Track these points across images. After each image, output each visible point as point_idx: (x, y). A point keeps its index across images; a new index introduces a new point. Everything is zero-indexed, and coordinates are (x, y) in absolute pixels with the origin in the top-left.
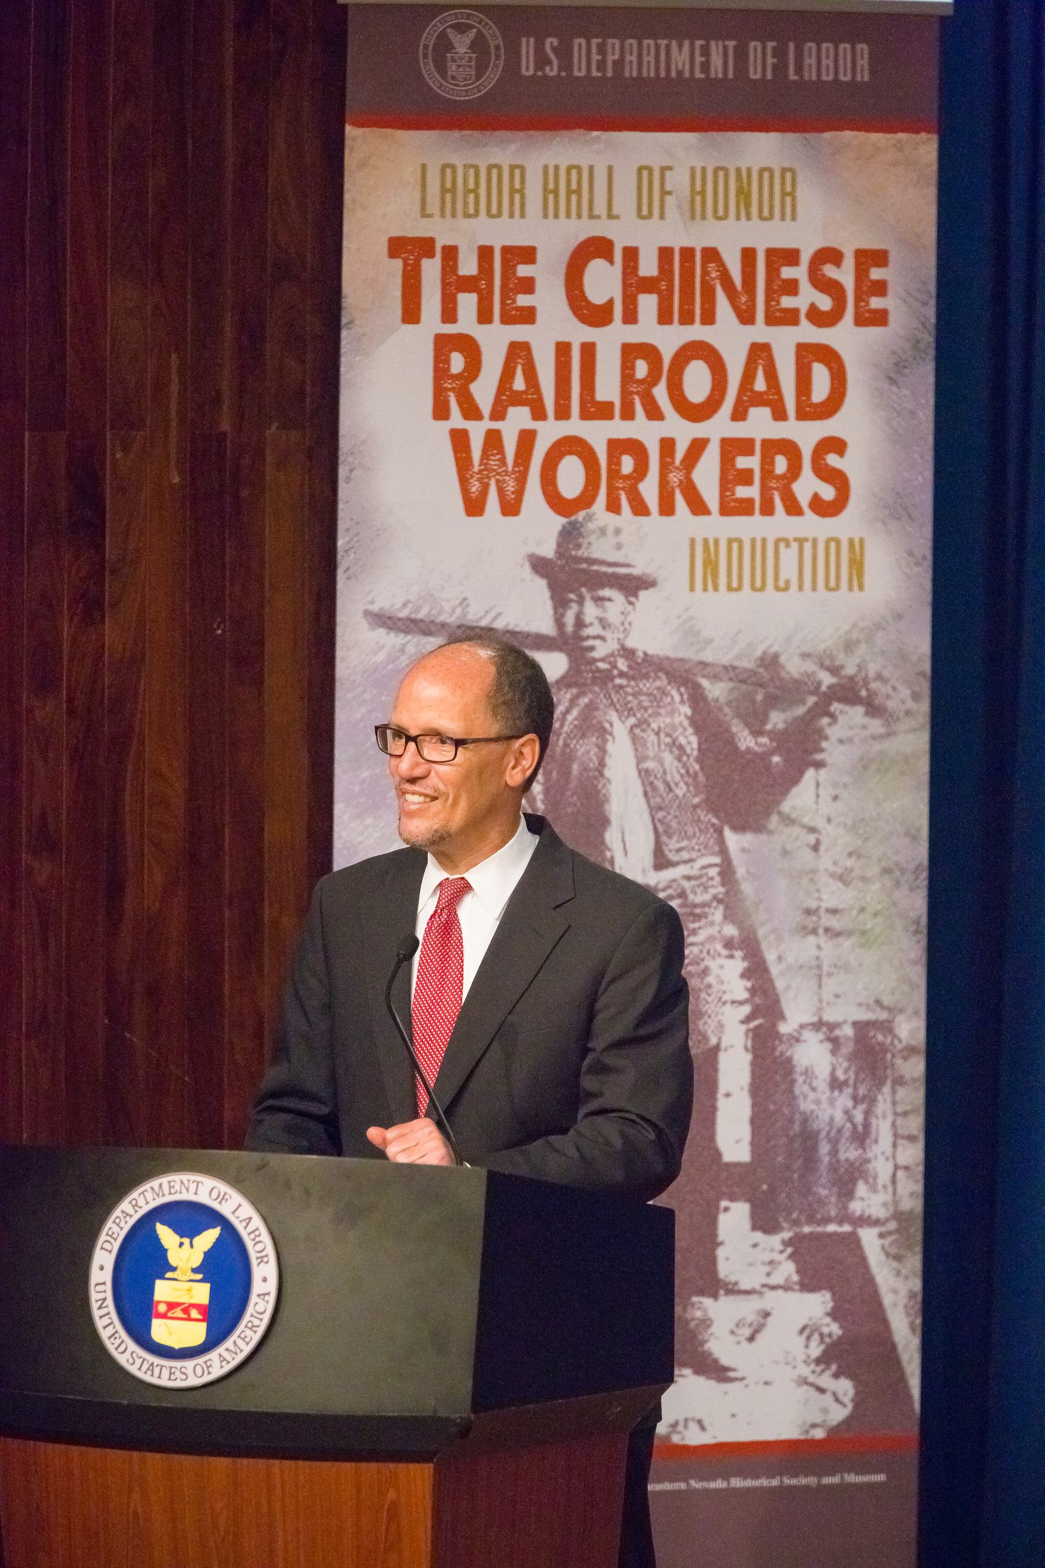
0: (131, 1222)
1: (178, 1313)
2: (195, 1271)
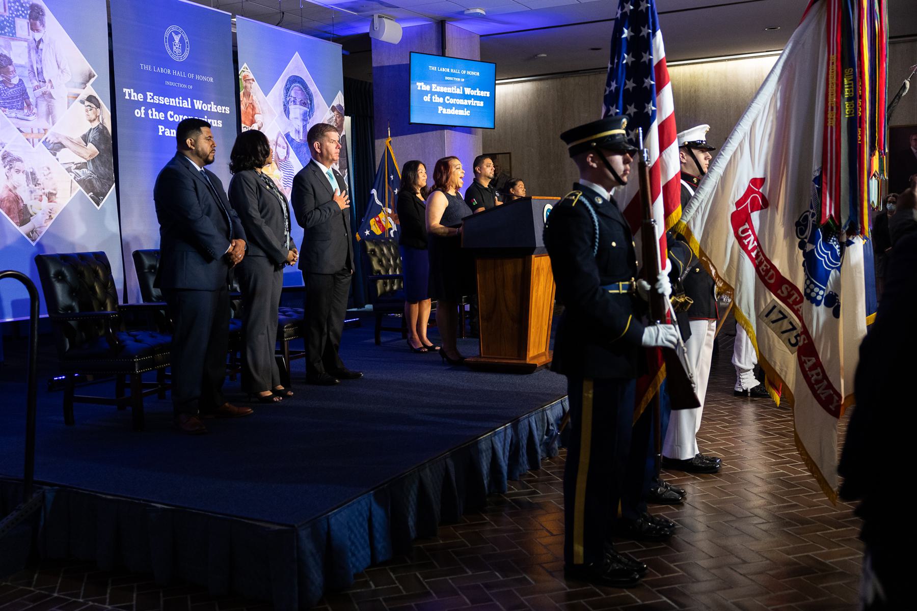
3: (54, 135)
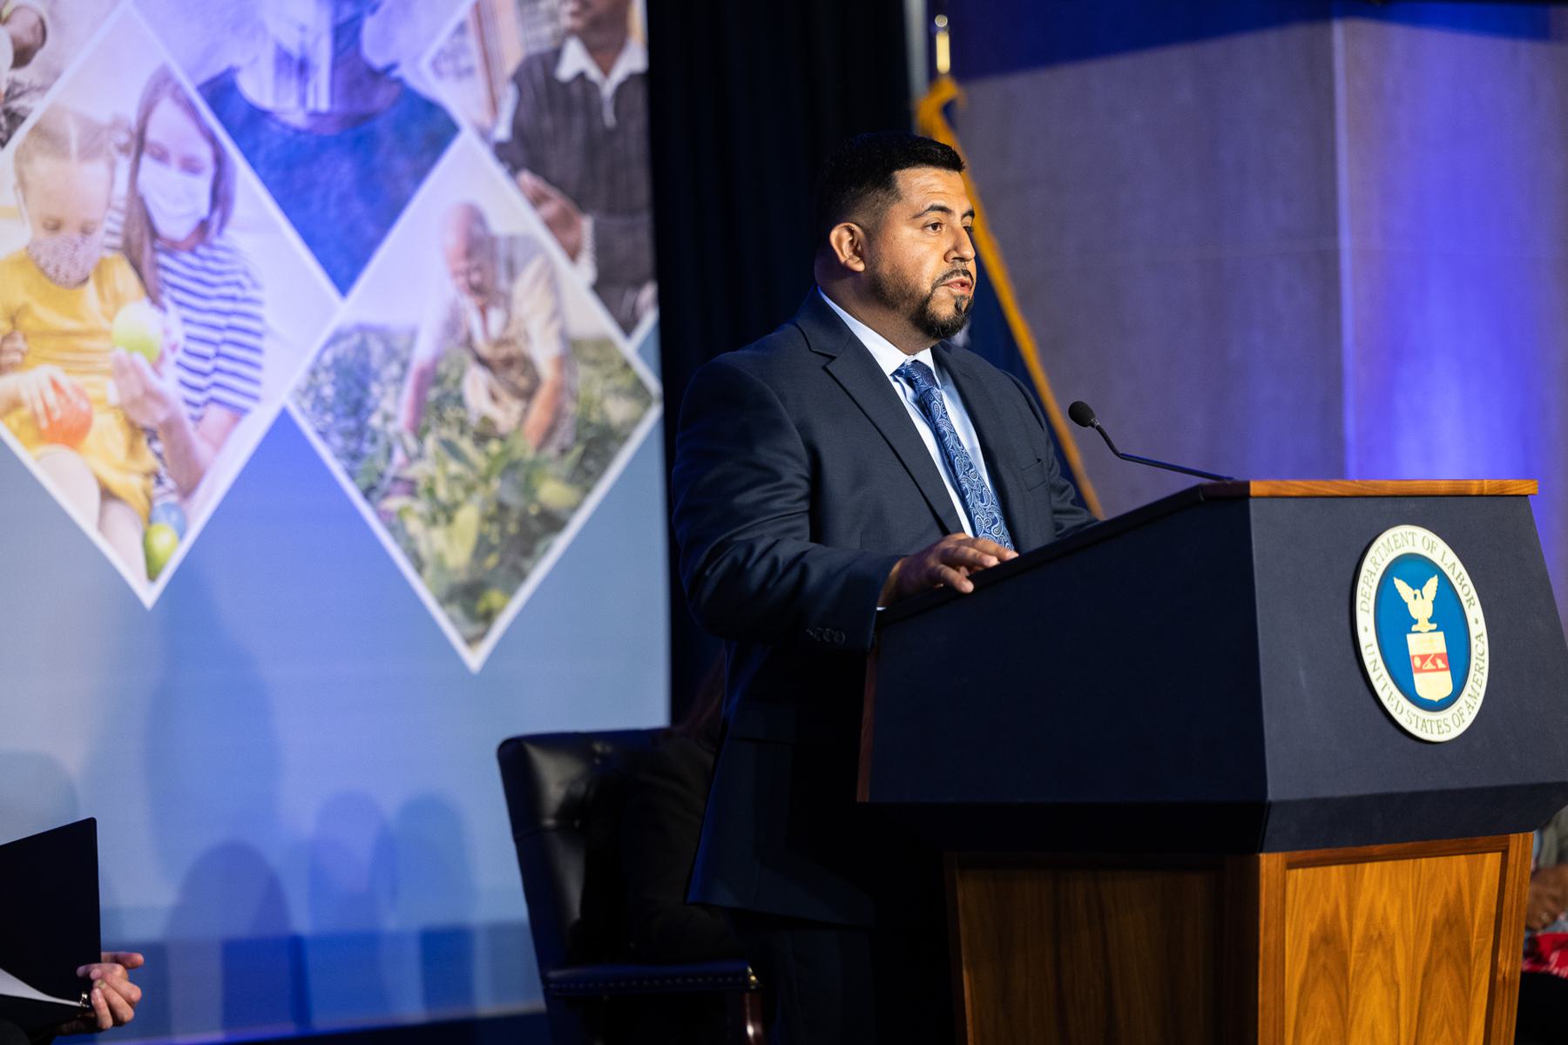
2: (1431, 621)
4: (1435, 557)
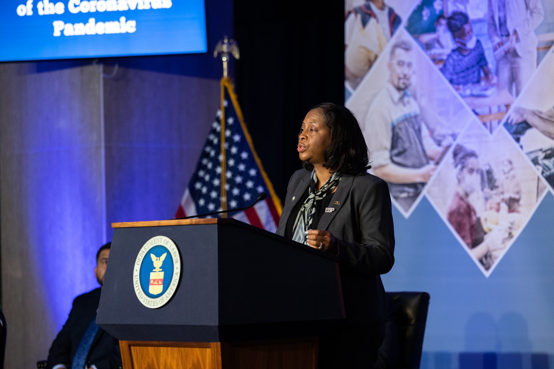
0: (145, 254)
1: (156, 283)
2: (160, 268)
3: (519, 111)
4: (167, 247)
